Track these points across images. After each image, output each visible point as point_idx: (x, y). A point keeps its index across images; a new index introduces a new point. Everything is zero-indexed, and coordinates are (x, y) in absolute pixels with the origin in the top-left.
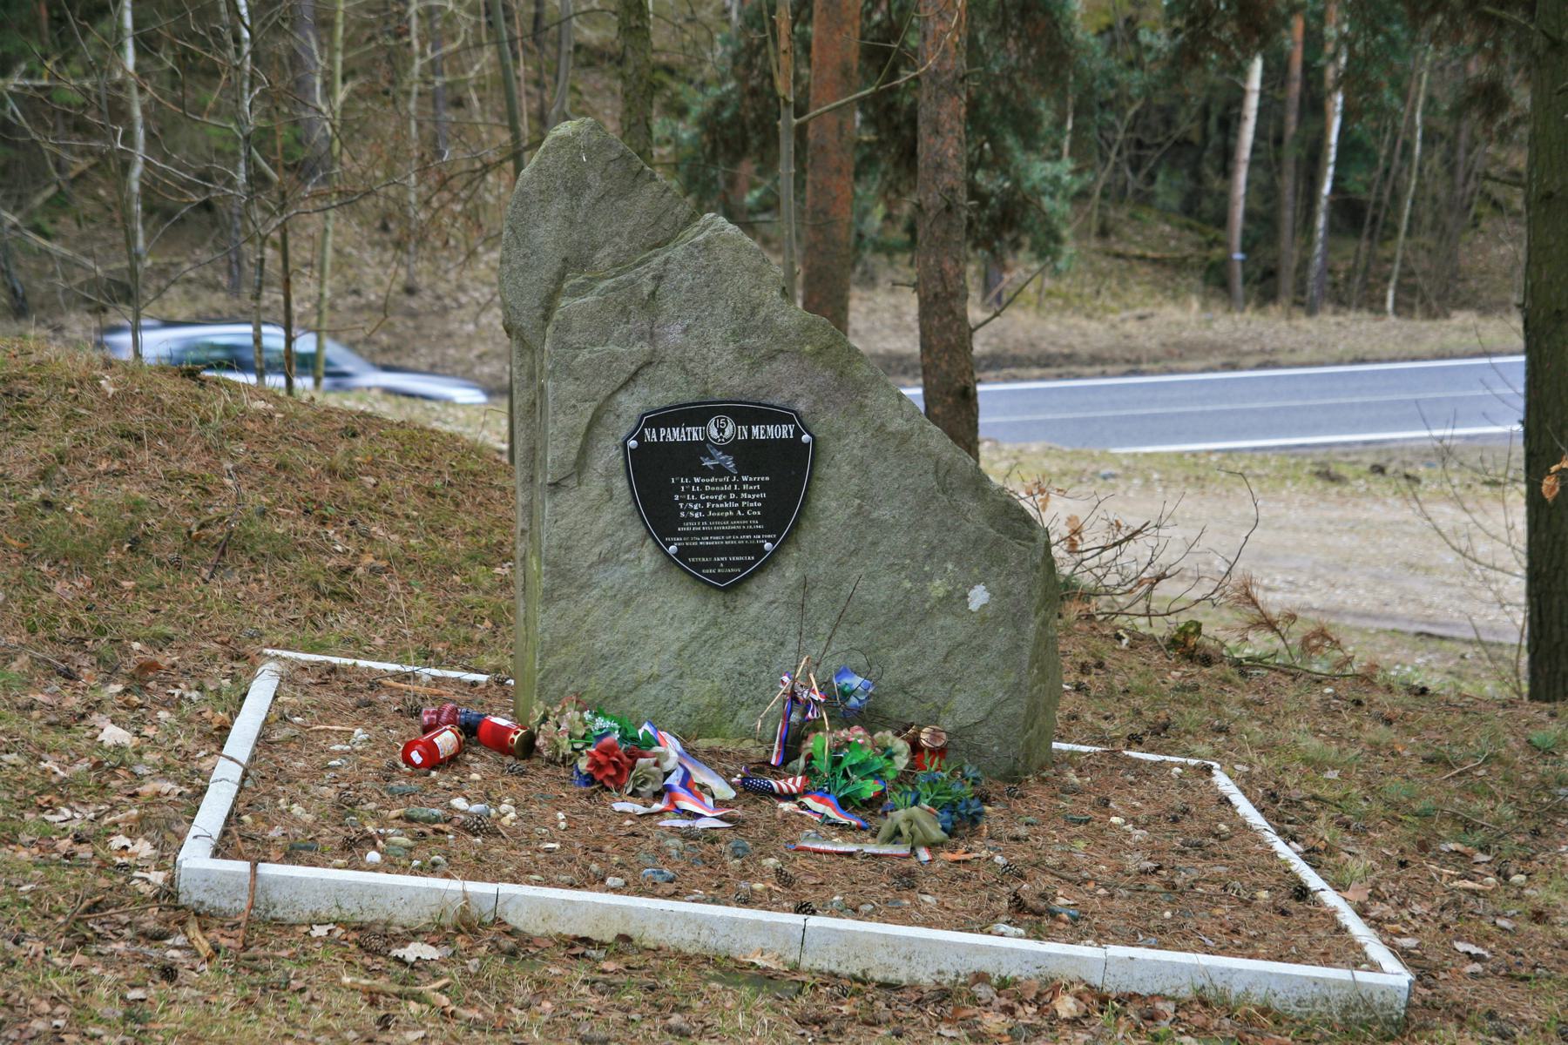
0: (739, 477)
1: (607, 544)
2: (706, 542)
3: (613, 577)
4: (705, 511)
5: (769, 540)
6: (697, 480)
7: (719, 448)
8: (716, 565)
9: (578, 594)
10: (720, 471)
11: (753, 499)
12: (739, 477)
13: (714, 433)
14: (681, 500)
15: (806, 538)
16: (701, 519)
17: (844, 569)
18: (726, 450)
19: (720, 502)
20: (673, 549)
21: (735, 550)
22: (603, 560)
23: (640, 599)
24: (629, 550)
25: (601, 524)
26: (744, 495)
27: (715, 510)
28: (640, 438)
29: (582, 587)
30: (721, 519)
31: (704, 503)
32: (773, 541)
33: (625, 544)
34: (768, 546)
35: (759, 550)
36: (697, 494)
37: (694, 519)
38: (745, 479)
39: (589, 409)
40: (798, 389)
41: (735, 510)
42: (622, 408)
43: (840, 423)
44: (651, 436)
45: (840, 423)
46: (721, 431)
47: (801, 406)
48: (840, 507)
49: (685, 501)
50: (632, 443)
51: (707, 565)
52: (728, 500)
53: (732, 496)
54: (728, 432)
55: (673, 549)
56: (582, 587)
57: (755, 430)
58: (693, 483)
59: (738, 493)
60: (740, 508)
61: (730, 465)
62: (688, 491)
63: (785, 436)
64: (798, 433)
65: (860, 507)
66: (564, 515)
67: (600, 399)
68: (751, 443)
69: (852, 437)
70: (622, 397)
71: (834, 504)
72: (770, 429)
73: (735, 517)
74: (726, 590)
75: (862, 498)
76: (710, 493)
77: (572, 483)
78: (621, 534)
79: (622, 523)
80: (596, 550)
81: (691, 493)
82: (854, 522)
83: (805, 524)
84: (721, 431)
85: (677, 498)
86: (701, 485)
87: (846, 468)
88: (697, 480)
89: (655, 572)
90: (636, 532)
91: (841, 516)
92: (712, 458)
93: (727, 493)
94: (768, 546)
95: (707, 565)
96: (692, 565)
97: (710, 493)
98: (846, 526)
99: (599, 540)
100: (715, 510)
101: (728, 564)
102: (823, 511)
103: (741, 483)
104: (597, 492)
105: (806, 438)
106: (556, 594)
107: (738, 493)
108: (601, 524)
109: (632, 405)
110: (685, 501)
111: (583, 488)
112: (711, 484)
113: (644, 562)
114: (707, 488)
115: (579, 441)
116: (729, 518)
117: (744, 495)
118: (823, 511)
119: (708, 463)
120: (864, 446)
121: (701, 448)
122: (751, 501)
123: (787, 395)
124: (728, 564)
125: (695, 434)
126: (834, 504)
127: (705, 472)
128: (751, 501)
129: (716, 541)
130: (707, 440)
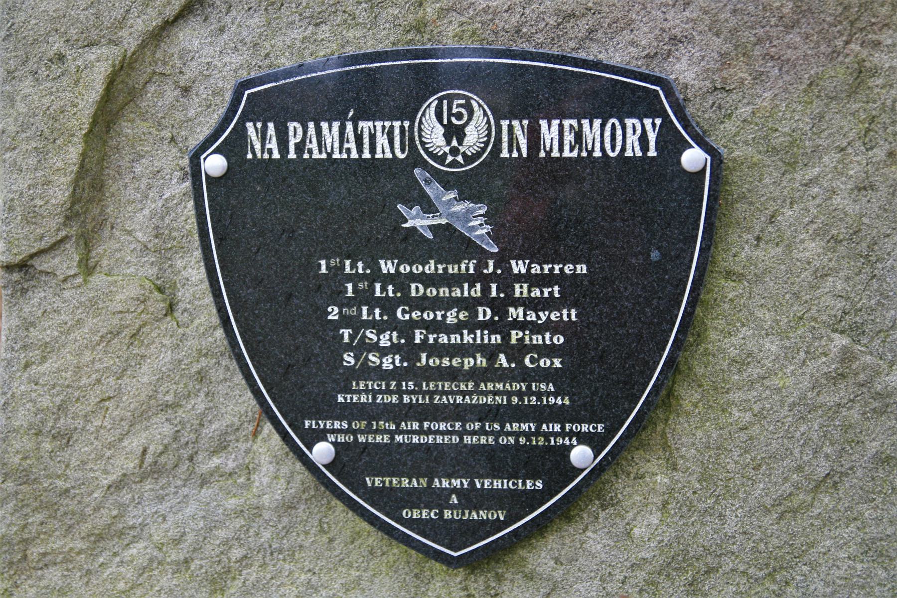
0: (502, 260)
1: (160, 430)
2: (411, 434)
3: (179, 512)
4: (410, 351)
5: (583, 438)
6: (387, 267)
7: (447, 181)
8: (439, 499)
9: (92, 552)
10: (451, 242)
11: (544, 328)
12: (502, 260)
13: (434, 135)
14: (345, 321)
15: (690, 430)
16: (396, 374)
17: (796, 526)
18: (467, 185)
19: (451, 330)
20: (322, 452)
21: (494, 461)
22: (152, 469)
23: (252, 574)
24: (221, 447)
25: (145, 375)
26: (516, 313)
27: (437, 350)
28: (234, 148)
29: (99, 538)
30: (453, 374)
31: (406, 329)
32: (595, 442)
33: (213, 429)
34: (581, 455)
35: (556, 465)
36: (389, 306)
37: (379, 373)
38: (518, 267)
39: (98, 65)
40: (676, 21)
41: (491, 353)
42: (192, 70)
43: (795, 120)
44: (261, 142)
45: (795, 120)
46: (454, 132)
47: (683, 71)
48: (788, 354)
49: (357, 324)
50: (215, 164)
51: (413, 498)
52: (472, 325)
53: (484, 314)
54: (473, 137)
55: (322, 452)
56: (99, 538)
57: (549, 132)
58: (376, 275)
59: (499, 307)
60: (505, 346)
61: (479, 229)
62: (365, 298)
63: (633, 149)
64: (672, 145)
65: (847, 356)
66: (47, 350)
67: (131, 44)
68: (540, 170)
69: (830, 160)
70: (191, 37)
71: (772, 346)
72: (592, 131)
73: (490, 373)
74: (471, 563)
75: (856, 331)
76: (423, 303)
77: (65, 263)
78: (200, 403)
79: (202, 376)
80: (134, 443)
81: (373, 302)
82: (829, 399)
83: (688, 397)
84: (454, 132)
85: (334, 313)
86: (400, 281)
87: (811, 249)
88: (387, 267)
89: (288, 506)
90: (236, 401)
91: (793, 381)
92: (429, 207)
93: (469, 304)
94: (581, 455)
95: (413, 498)
96: (373, 495)
97: (423, 303)
98: (803, 408)
99: (140, 417)
100: (437, 350)
101: (471, 499)
102: (741, 364)
103: (507, 280)
104: (133, 291)
105: (693, 158)
106: (34, 552)
107: (499, 307)
108: (145, 375)
109: (216, 58)
110: (357, 324)
111: (97, 279)
112: (428, 280)
113: (261, 479)
114: (416, 290)
115: (74, 153)
116: (475, 374)
117: (516, 313)
118: (741, 364)
119: (417, 220)
120: (863, 188)
121: (395, 180)
122: (536, 328)
123: (645, 37)
124: (471, 499)
125: (382, 140)
126: (772, 346)
127: (410, 246)
128: (536, 328)
129: (441, 434)
130: (415, 160)
